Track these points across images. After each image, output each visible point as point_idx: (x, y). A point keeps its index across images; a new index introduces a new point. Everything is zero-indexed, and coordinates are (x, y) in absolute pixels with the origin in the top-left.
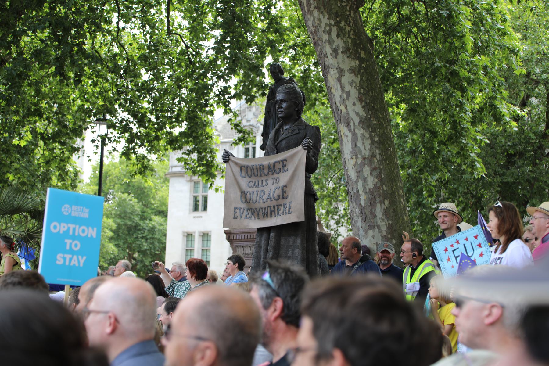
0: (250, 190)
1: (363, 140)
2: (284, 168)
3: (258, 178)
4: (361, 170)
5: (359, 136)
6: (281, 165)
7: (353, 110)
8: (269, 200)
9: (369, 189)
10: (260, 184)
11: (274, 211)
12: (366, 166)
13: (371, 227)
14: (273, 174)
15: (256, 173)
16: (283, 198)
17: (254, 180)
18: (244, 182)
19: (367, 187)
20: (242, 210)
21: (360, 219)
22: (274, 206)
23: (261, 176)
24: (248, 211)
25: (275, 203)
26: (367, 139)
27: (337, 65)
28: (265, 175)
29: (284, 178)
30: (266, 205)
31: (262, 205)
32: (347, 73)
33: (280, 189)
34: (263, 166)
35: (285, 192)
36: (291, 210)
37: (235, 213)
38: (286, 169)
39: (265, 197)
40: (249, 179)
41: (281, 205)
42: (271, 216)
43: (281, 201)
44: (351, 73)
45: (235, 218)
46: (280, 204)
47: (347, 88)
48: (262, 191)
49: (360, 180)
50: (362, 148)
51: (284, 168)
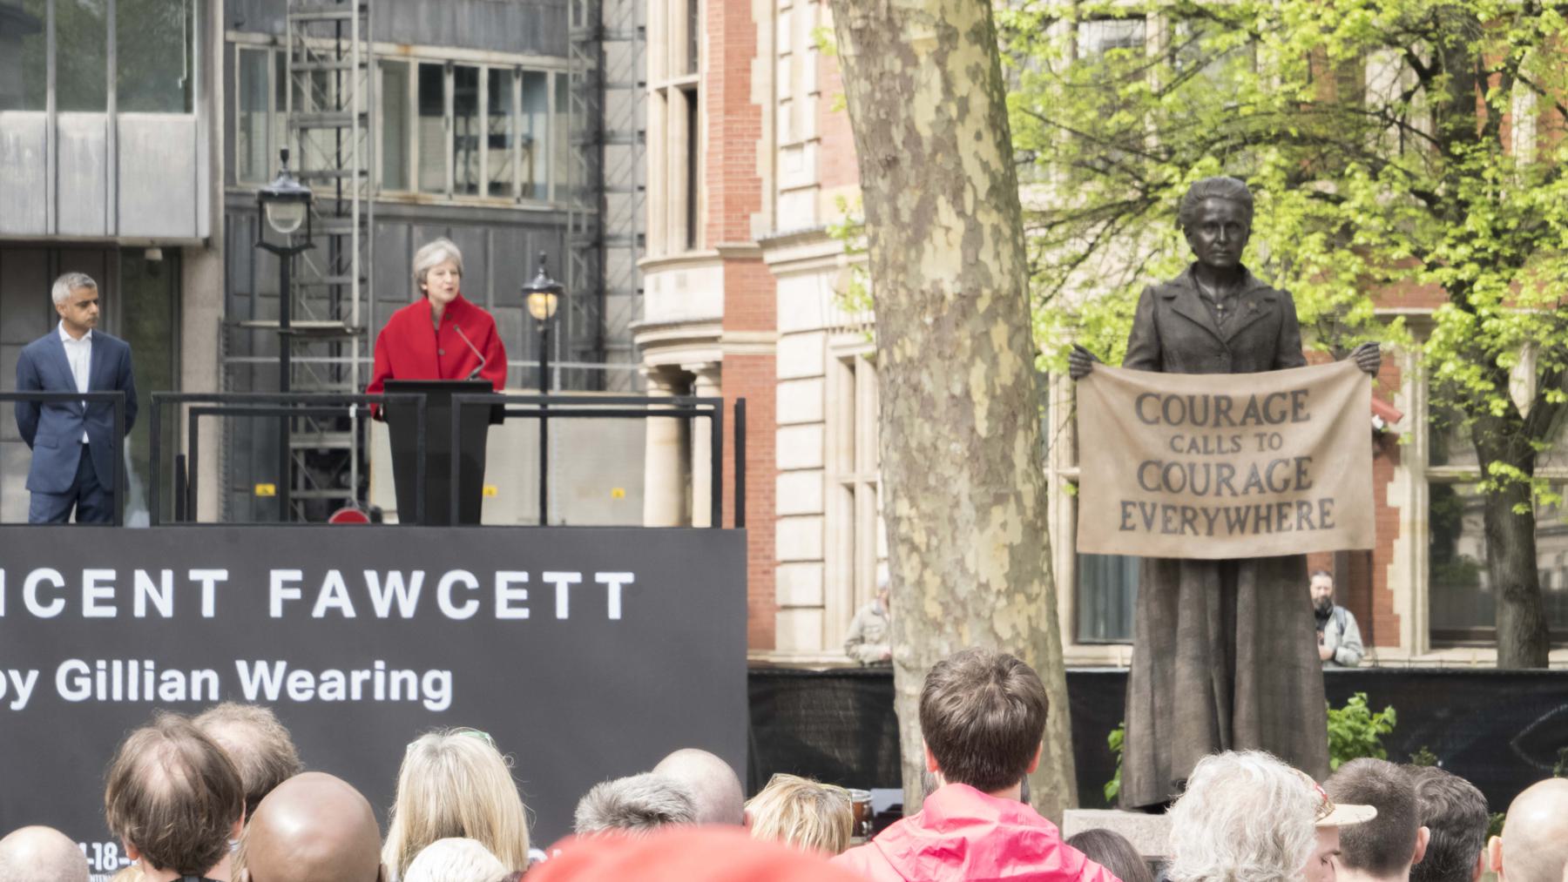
0: (1184, 459)
1: (996, 243)
2: (1295, 413)
3: (1205, 430)
4: (987, 333)
5: (987, 231)
6: (1288, 404)
7: (976, 154)
8: (1253, 490)
9: (1003, 387)
10: (1213, 445)
11: (1268, 519)
12: (1000, 320)
13: (1000, 499)
14: (1259, 422)
15: (1200, 417)
16: (1300, 487)
17: (1189, 433)
18: (1154, 440)
19: (997, 381)
20: (1148, 509)
21: (966, 474)
22: (1269, 507)
23: (1217, 424)
24: (1170, 513)
25: (1271, 498)
26: (1006, 241)
27: (938, 16)
28: (1232, 424)
29: (1299, 438)
30: (1241, 501)
31: (1227, 500)
32: (963, 42)
33: (1293, 464)
34: (1229, 400)
35: (1305, 473)
36: (1328, 521)
37: (1126, 516)
38: (1302, 413)
39: (1239, 481)
40: (1174, 431)
41: (1289, 505)
42: (1256, 530)
43: (1290, 495)
44: (975, 42)
45: (1123, 527)
46: (1288, 499)
47: (963, 86)
48: (1220, 466)
49: (978, 361)
50: (993, 268)
51: (1295, 413)
